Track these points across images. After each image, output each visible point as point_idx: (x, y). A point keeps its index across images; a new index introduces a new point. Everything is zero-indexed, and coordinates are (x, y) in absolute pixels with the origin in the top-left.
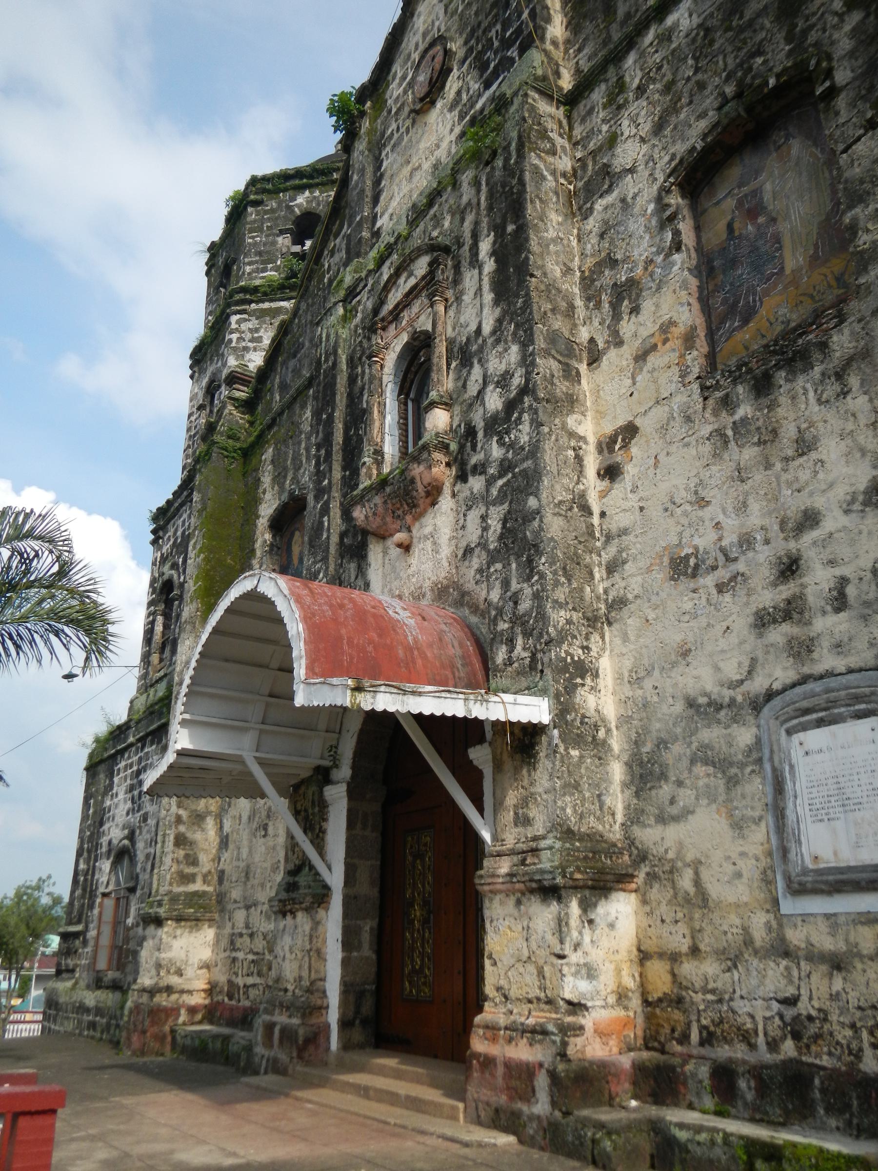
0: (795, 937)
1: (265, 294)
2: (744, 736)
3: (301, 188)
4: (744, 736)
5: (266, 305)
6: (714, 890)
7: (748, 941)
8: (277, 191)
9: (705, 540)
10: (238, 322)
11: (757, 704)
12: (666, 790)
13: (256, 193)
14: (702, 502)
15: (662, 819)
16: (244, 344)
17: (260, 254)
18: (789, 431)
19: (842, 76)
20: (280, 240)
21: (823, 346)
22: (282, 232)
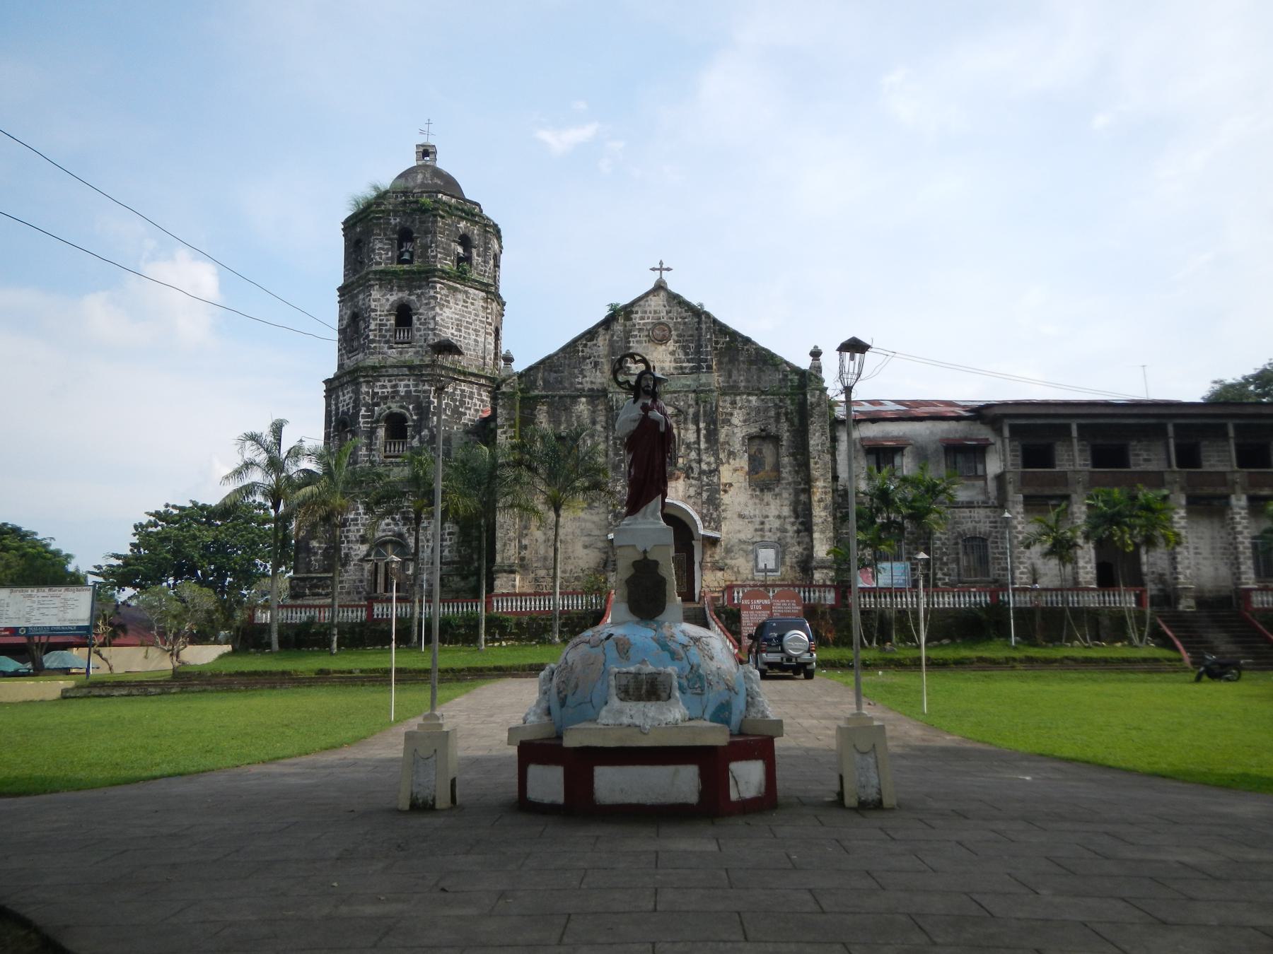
0: (756, 578)
1: (450, 277)
2: (751, 548)
3: (462, 218)
4: (751, 548)
5: (451, 283)
6: (741, 571)
7: (747, 579)
8: (451, 215)
9: (746, 513)
10: (440, 288)
11: (754, 543)
12: (733, 554)
13: (442, 210)
14: (747, 506)
15: (731, 559)
16: (442, 302)
17: (444, 248)
18: (766, 500)
19: (784, 443)
20: (453, 244)
21: (774, 490)
22: (454, 241)
